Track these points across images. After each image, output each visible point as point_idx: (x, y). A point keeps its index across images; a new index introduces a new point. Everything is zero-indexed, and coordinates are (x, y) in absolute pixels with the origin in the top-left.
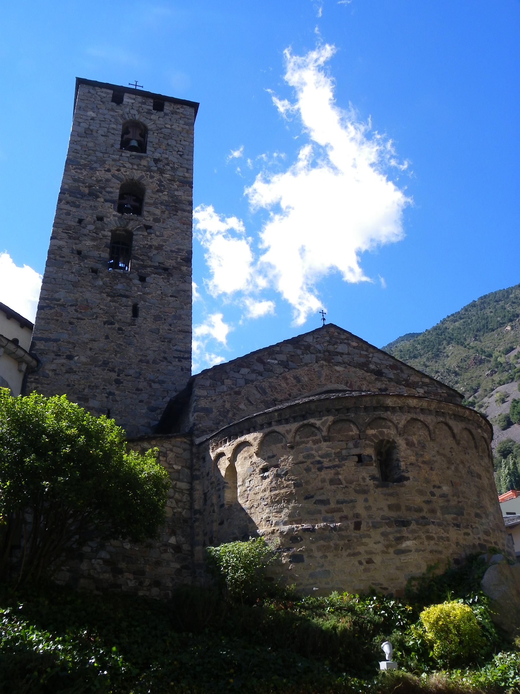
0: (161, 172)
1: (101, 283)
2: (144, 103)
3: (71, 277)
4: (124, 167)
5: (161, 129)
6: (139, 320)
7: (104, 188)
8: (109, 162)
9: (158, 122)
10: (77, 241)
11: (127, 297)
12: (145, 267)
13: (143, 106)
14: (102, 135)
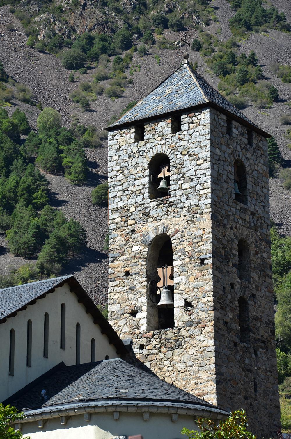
0: (256, 228)
1: (239, 358)
2: (242, 134)
3: (226, 352)
4: (238, 223)
5: (253, 171)
6: (258, 397)
7: (231, 250)
8: (232, 218)
9: (251, 162)
10: (224, 312)
11: (251, 371)
12: (256, 340)
13: (243, 139)
14: (225, 181)
